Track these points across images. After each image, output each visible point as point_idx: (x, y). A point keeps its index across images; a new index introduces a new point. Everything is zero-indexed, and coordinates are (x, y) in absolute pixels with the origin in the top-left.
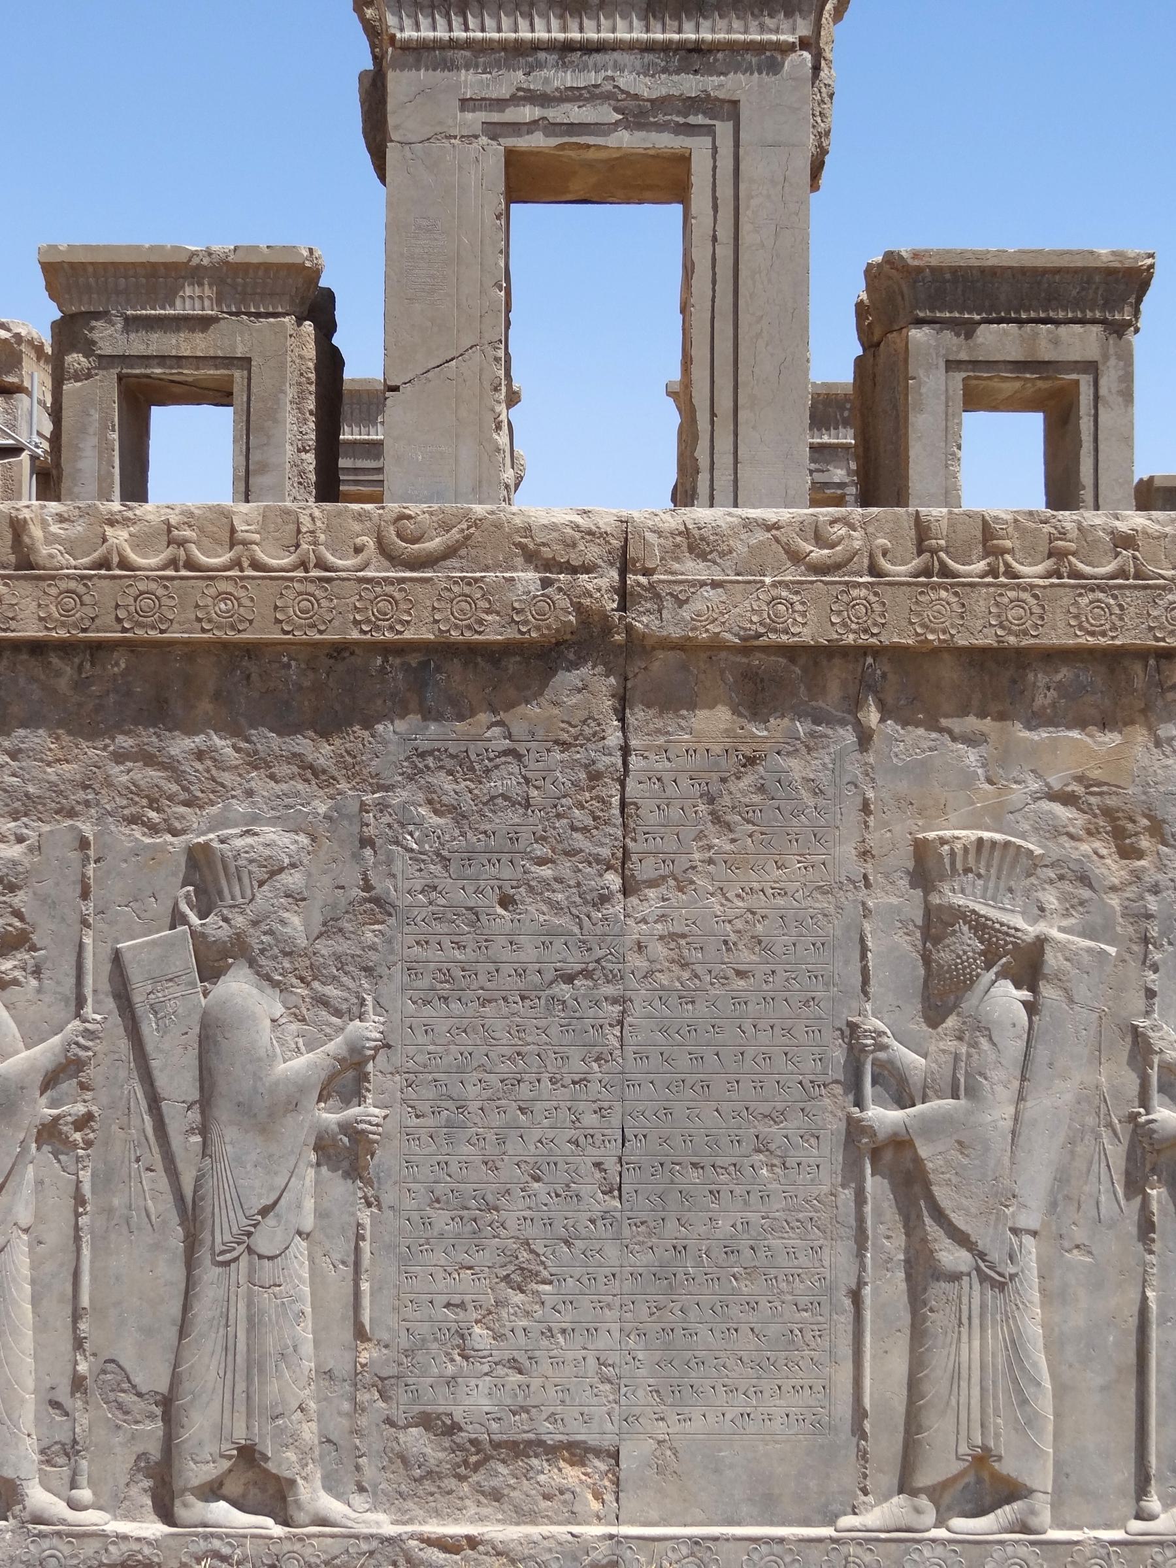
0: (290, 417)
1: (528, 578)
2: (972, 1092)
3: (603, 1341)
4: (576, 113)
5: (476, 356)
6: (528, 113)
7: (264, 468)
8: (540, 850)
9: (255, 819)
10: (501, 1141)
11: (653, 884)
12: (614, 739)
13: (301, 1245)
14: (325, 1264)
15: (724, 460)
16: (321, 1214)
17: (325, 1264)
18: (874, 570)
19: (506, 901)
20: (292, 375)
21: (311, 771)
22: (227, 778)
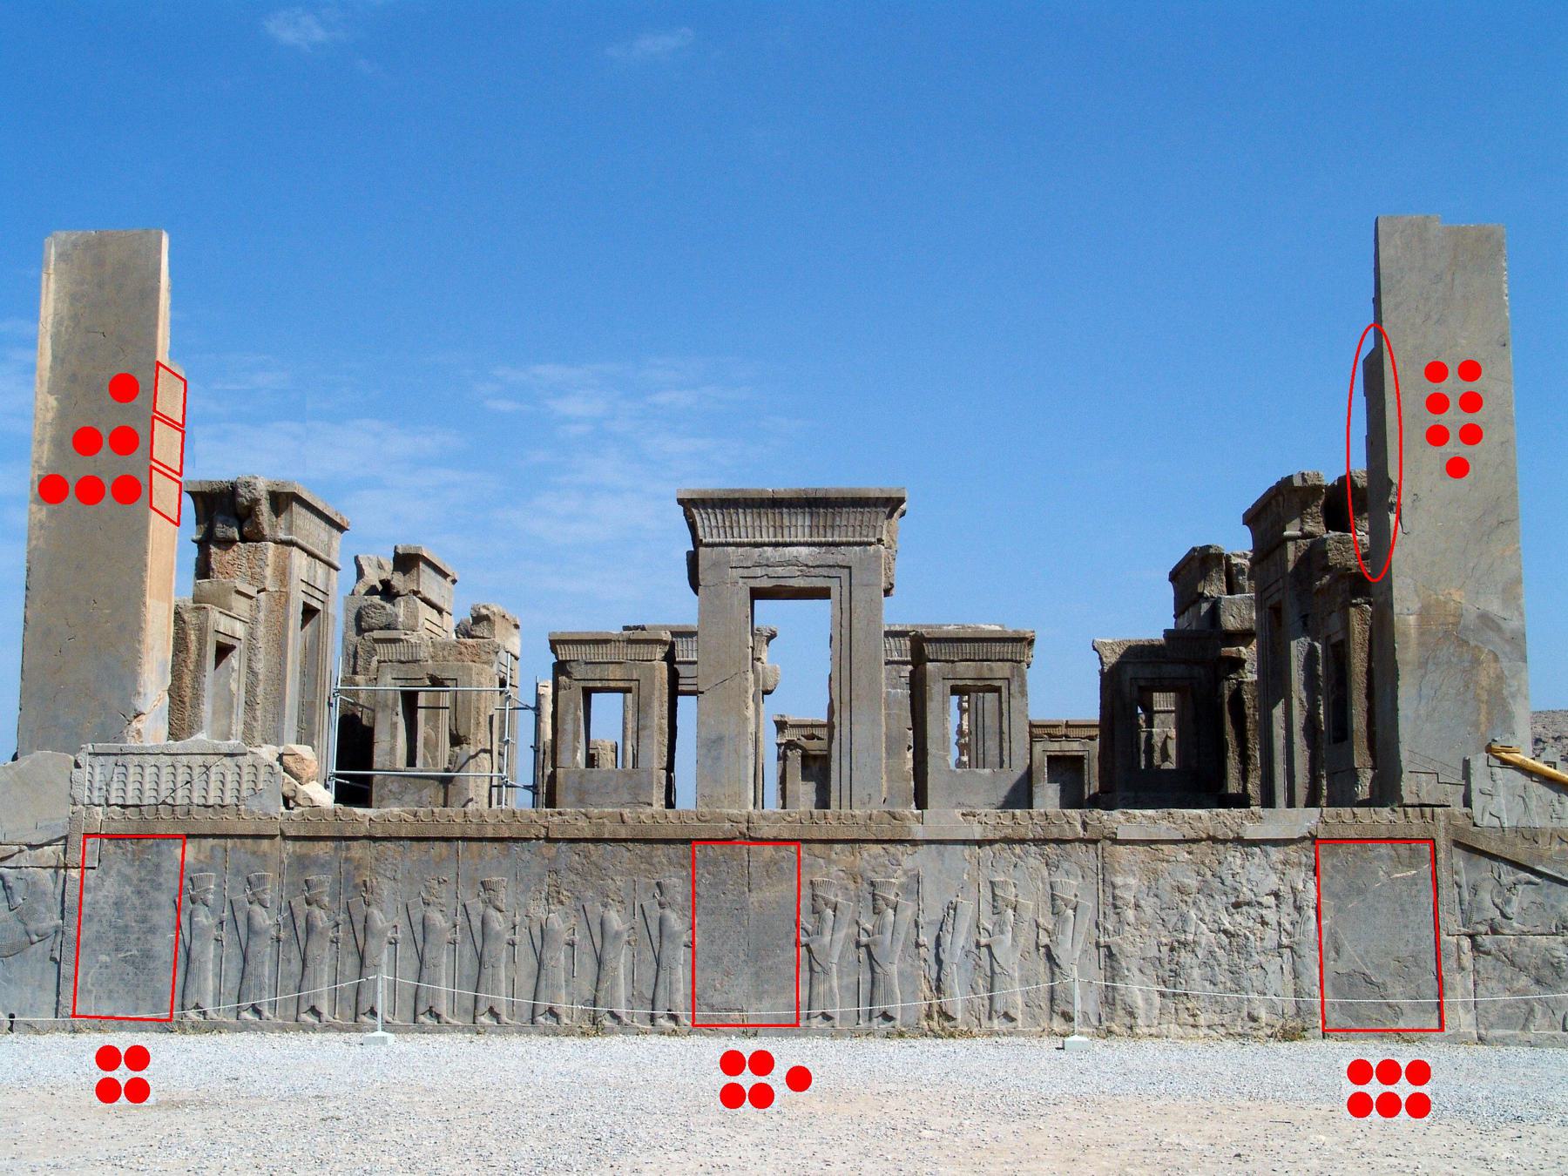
0: (656, 704)
1: (727, 825)
2: (822, 933)
3: (744, 987)
4: (780, 571)
5: (737, 679)
6: (759, 572)
7: (645, 728)
8: (731, 882)
9: (670, 876)
10: (723, 945)
11: (755, 888)
12: (747, 859)
13: (680, 966)
14: (686, 971)
15: (846, 723)
16: (685, 960)
17: (686, 971)
18: (801, 823)
19: (724, 893)
20: (657, 684)
21: (683, 866)
22: (665, 867)
